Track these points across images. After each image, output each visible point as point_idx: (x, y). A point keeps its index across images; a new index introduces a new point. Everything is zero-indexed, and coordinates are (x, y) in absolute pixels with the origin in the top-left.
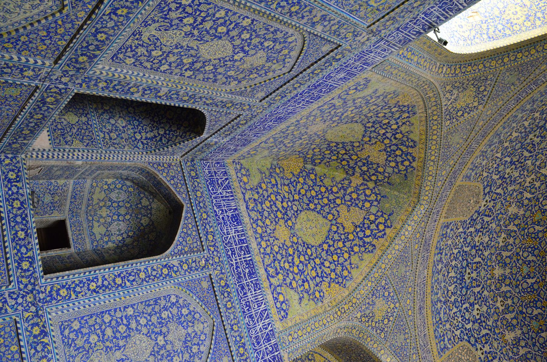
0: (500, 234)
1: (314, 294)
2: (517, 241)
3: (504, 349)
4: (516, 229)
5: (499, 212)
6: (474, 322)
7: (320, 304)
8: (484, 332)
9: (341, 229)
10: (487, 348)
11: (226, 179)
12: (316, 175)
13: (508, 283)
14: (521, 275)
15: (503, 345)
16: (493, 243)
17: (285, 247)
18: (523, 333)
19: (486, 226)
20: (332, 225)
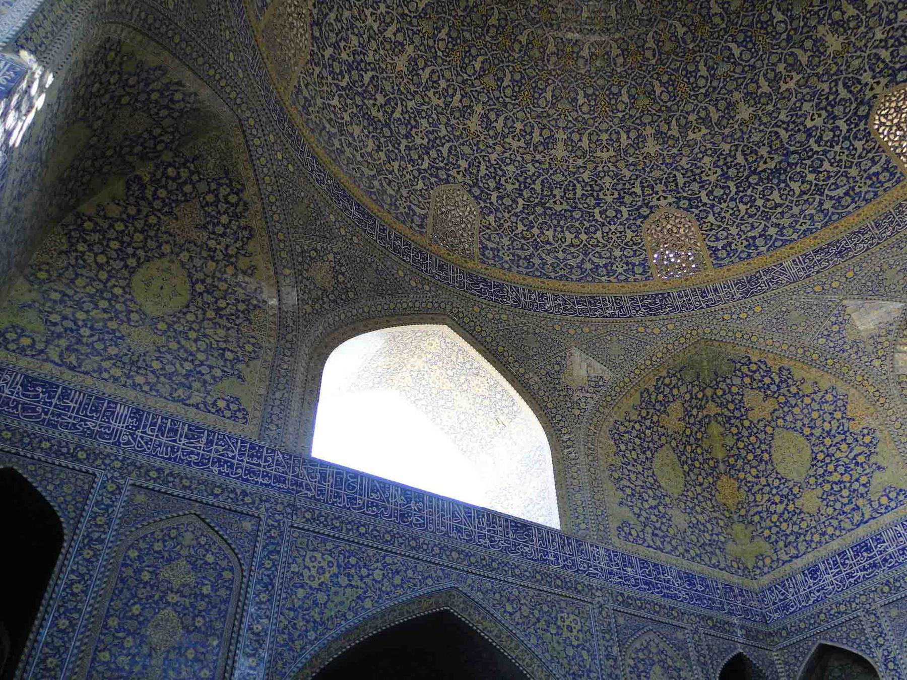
0: (691, 143)
1: (867, 445)
4: (674, 121)
5: (663, 167)
6: (835, 118)
7: (878, 434)
8: (843, 93)
9: (776, 414)
10: (867, 77)
11: (776, 588)
12: (729, 457)
13: (754, 85)
14: (734, 71)
15: (852, 49)
17: (825, 497)
18: (819, 22)
19: (689, 174)
20: (777, 426)
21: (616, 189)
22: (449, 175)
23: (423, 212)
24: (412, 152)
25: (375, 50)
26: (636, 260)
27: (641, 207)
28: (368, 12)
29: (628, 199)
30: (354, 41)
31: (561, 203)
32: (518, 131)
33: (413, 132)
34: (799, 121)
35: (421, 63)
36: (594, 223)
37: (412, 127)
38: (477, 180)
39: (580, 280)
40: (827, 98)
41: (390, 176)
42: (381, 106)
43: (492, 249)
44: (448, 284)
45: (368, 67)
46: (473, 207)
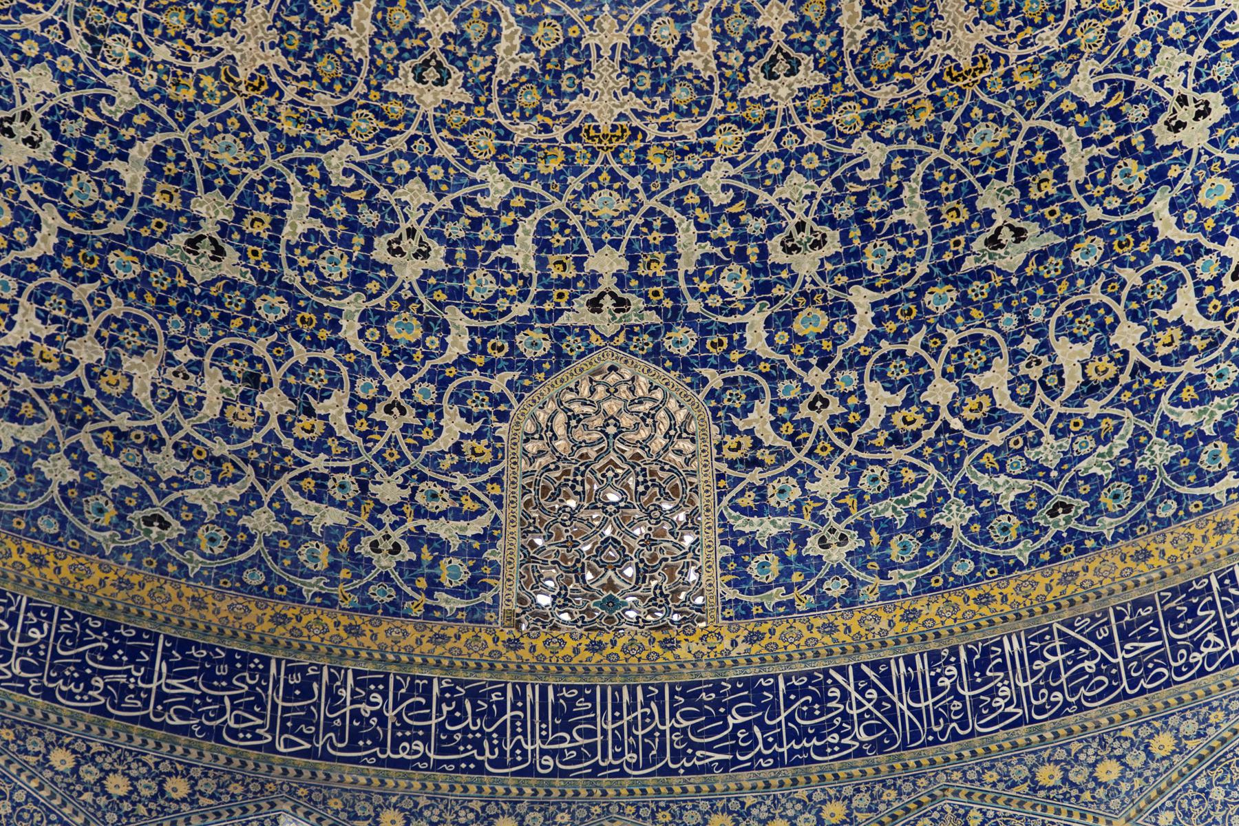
21: (1212, 86)
23: (475, 527)
24: (391, 328)
25: (135, 62)
31: (1019, 234)
32: (778, 37)
33: (380, 253)
36: (1158, 261)
37: (369, 235)
38: (674, 294)
39: (1128, 533)
41: (319, 463)
42: (224, 230)
43: (777, 543)
44: (596, 768)
45: (127, 133)
46: (682, 404)
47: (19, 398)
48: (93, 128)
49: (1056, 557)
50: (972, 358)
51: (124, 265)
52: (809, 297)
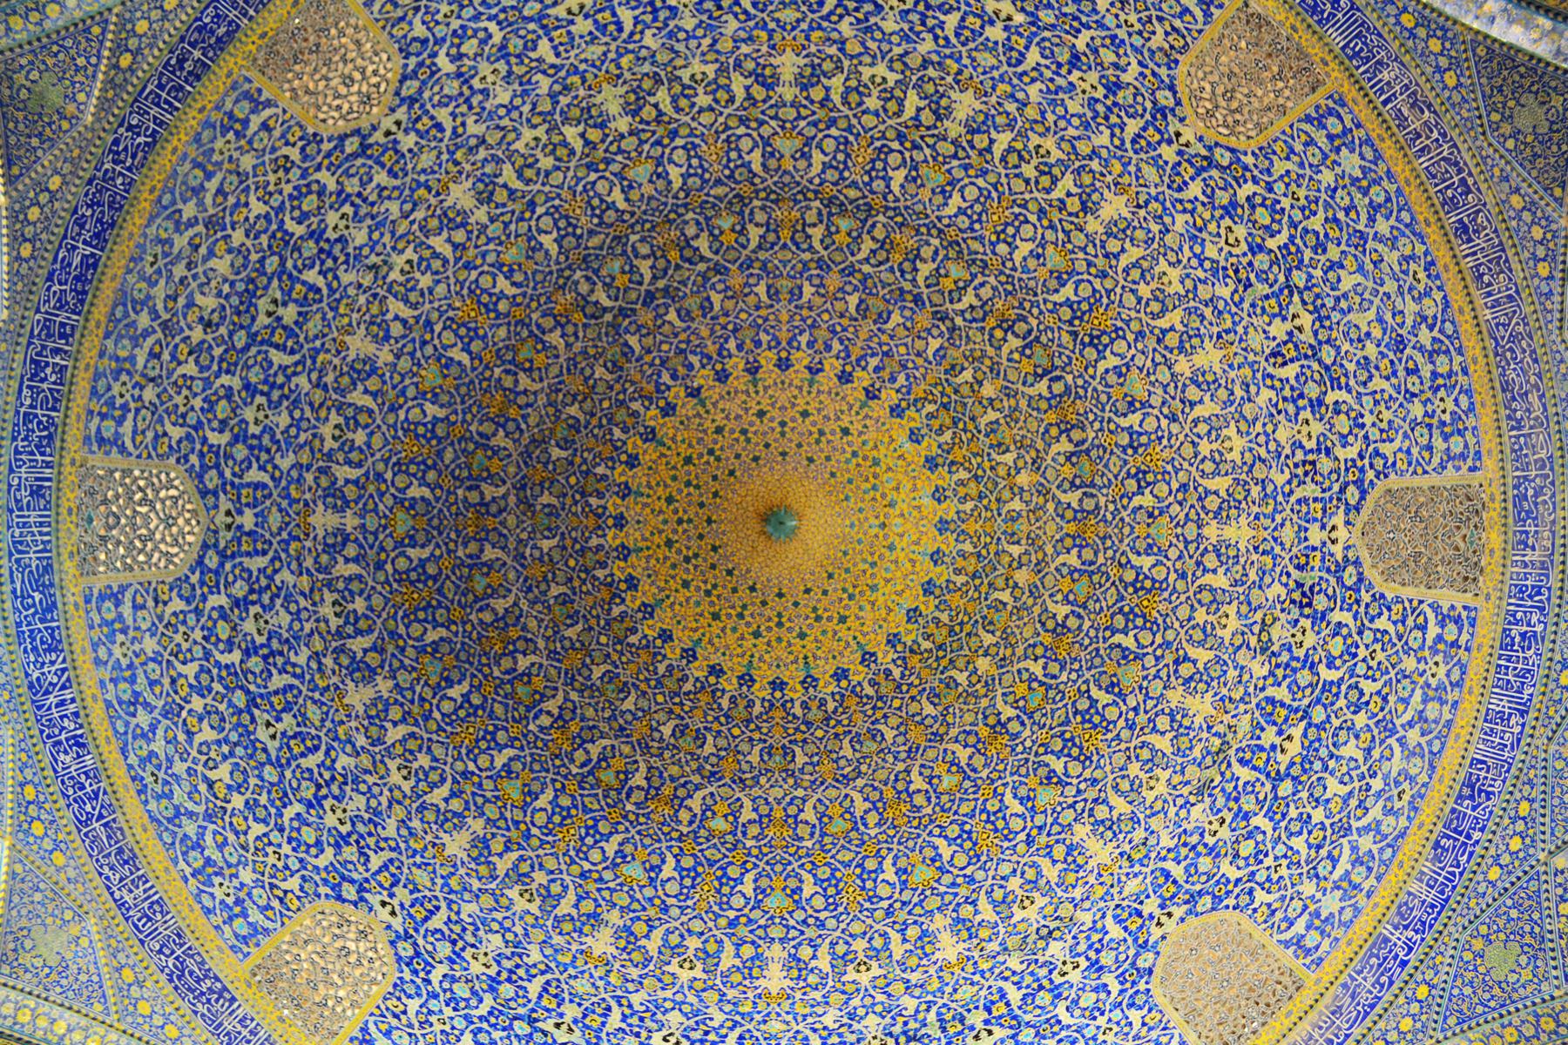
2: (551, 863)
3: (801, 1009)
4: (514, 855)
5: (439, 881)
13: (645, 929)
15: (786, 1005)
16: (519, 930)
19: (457, 929)
22: (215, 493)
23: (128, 444)
24: (223, 403)
26: (255, 916)
27: (352, 882)
28: (410, 253)
29: (350, 852)
30: (360, 237)
31: (273, 737)
32: (350, 607)
33: (259, 399)
34: (648, 1023)
35: (373, 384)
38: (233, 556)
40: (706, 1033)
41: (166, 356)
43: (120, 618)
44: (11, 511)
46: (182, 559)
47: (225, 196)
48: (335, 260)
49: (134, 779)
50: (215, 718)
51: (272, 264)
52: (234, 629)
